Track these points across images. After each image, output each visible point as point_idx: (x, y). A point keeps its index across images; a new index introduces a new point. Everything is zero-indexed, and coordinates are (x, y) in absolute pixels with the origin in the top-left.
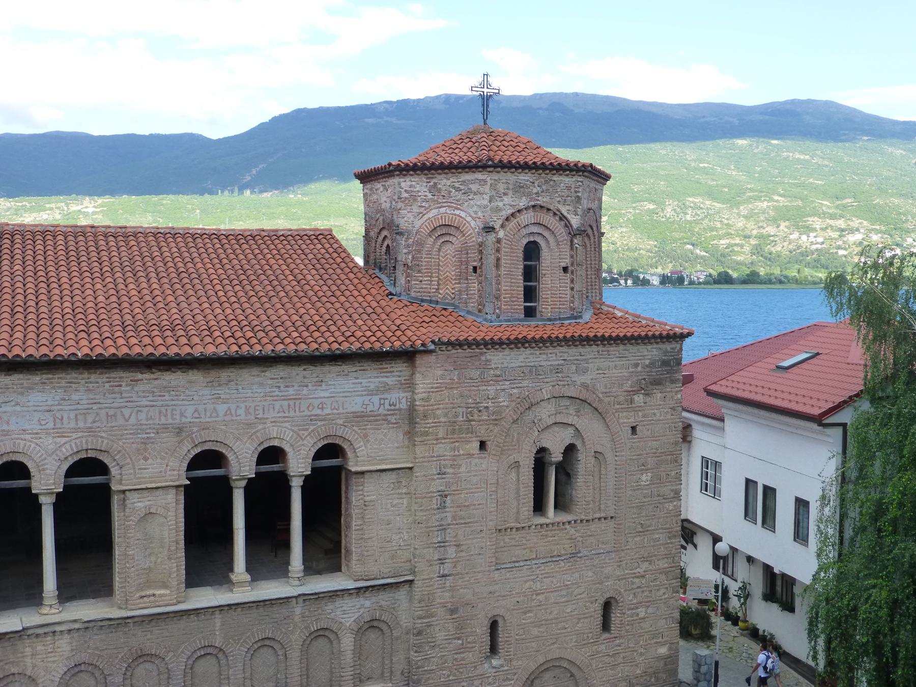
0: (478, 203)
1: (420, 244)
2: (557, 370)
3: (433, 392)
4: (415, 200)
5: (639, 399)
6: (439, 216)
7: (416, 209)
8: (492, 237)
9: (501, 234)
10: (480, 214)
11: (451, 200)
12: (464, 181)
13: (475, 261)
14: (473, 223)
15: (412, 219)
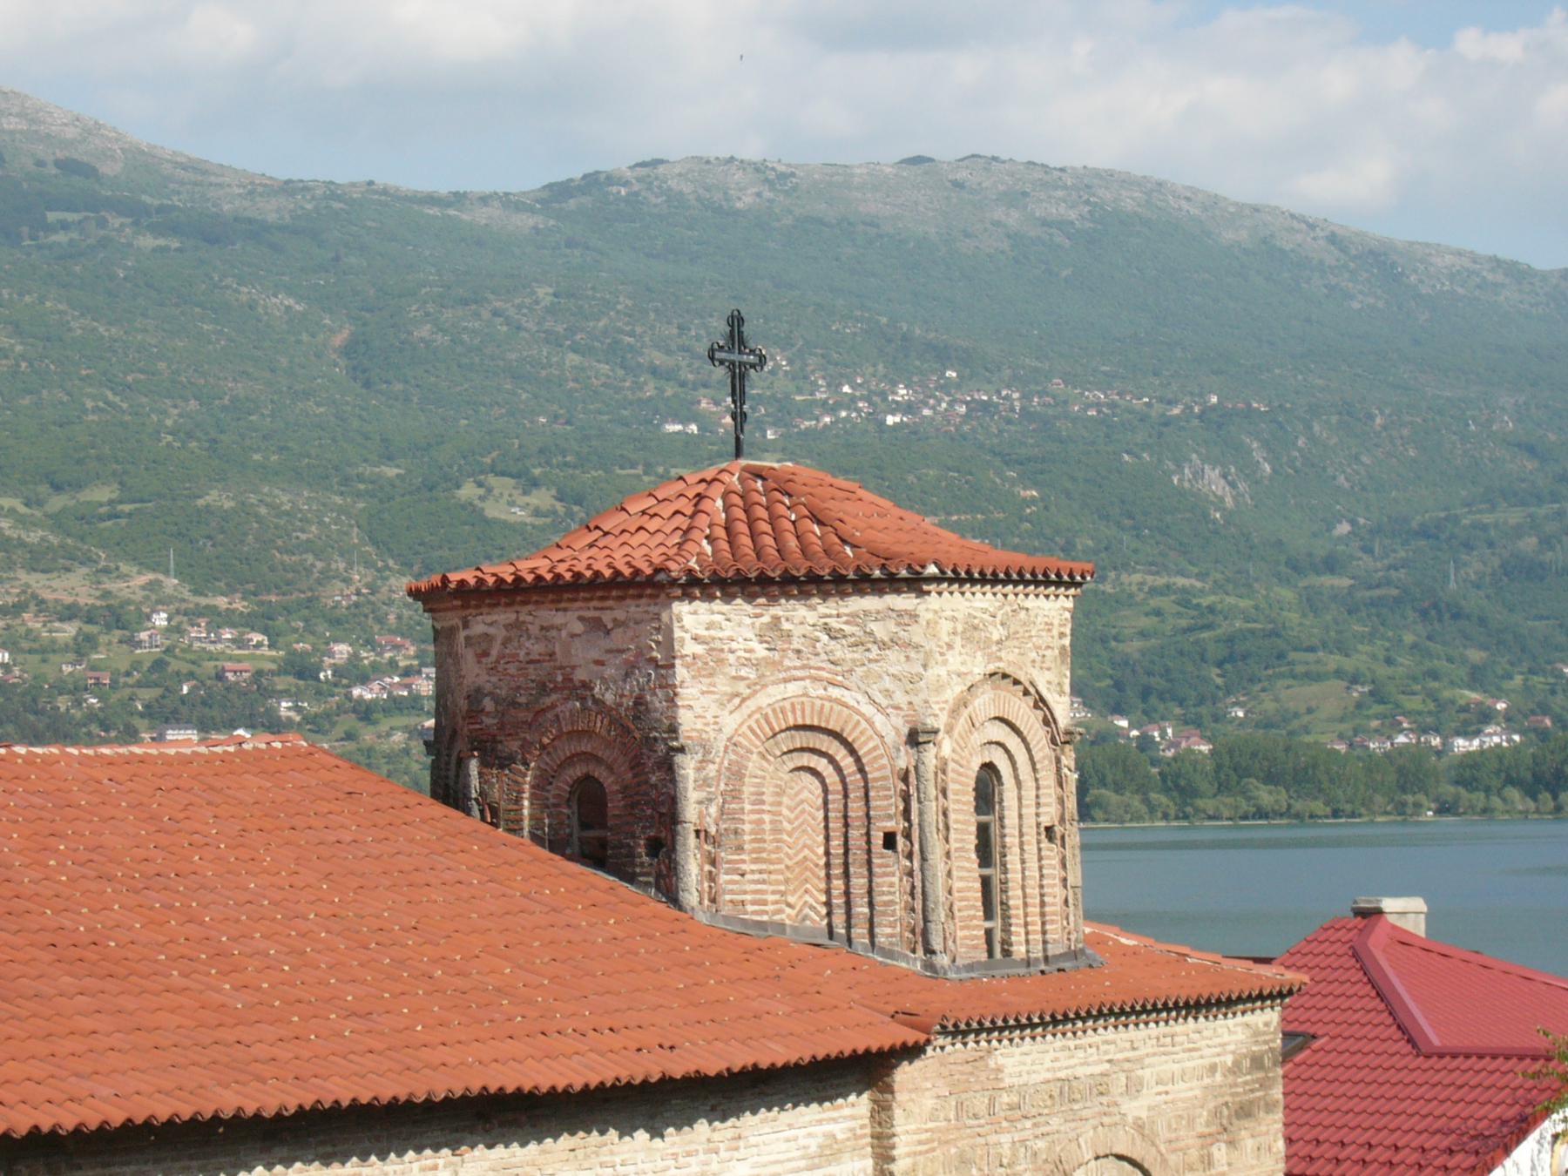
0: (892, 670)
1: (737, 774)
2: (1100, 1087)
3: (921, 1153)
4: (720, 662)
5: (1220, 1152)
6: (787, 705)
7: (723, 686)
8: (930, 756)
9: (947, 748)
10: (900, 698)
11: (814, 662)
12: (854, 615)
13: (890, 817)
14: (879, 720)
15: (714, 709)
